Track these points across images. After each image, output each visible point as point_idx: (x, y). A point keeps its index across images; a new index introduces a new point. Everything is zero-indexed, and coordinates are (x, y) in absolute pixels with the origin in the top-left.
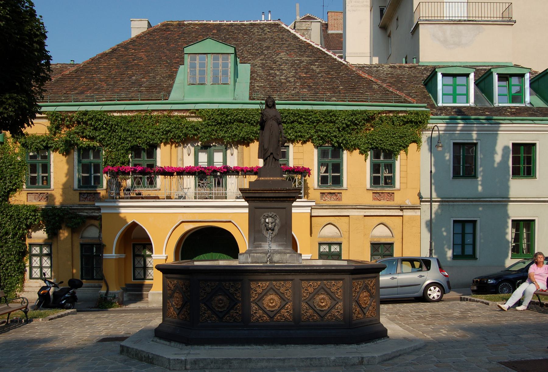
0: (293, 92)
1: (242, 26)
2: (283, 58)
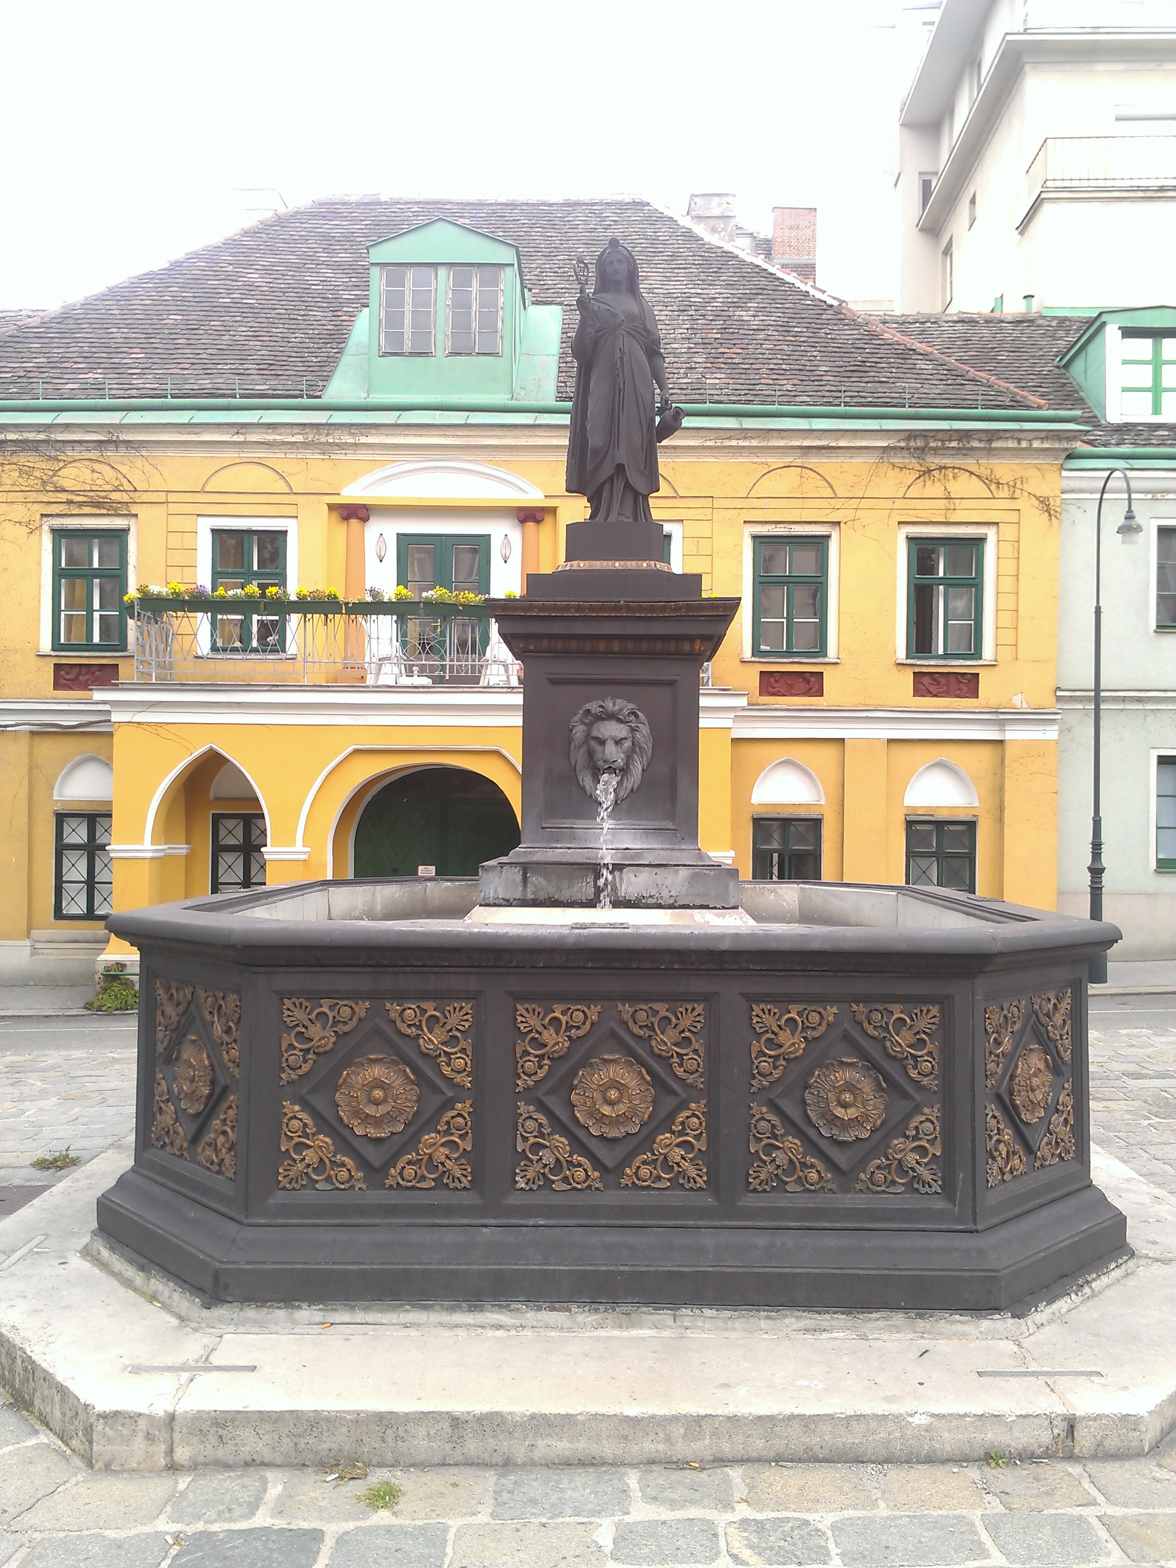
0: (686, 381)
1: (541, 208)
2: (656, 291)
